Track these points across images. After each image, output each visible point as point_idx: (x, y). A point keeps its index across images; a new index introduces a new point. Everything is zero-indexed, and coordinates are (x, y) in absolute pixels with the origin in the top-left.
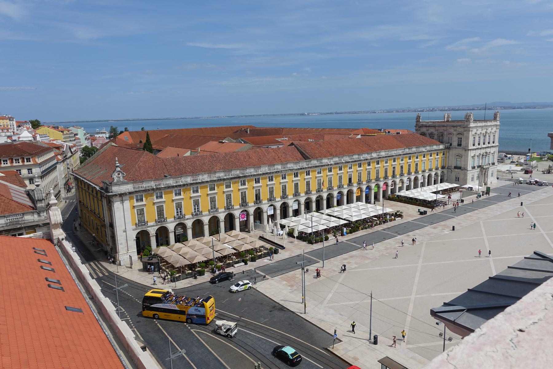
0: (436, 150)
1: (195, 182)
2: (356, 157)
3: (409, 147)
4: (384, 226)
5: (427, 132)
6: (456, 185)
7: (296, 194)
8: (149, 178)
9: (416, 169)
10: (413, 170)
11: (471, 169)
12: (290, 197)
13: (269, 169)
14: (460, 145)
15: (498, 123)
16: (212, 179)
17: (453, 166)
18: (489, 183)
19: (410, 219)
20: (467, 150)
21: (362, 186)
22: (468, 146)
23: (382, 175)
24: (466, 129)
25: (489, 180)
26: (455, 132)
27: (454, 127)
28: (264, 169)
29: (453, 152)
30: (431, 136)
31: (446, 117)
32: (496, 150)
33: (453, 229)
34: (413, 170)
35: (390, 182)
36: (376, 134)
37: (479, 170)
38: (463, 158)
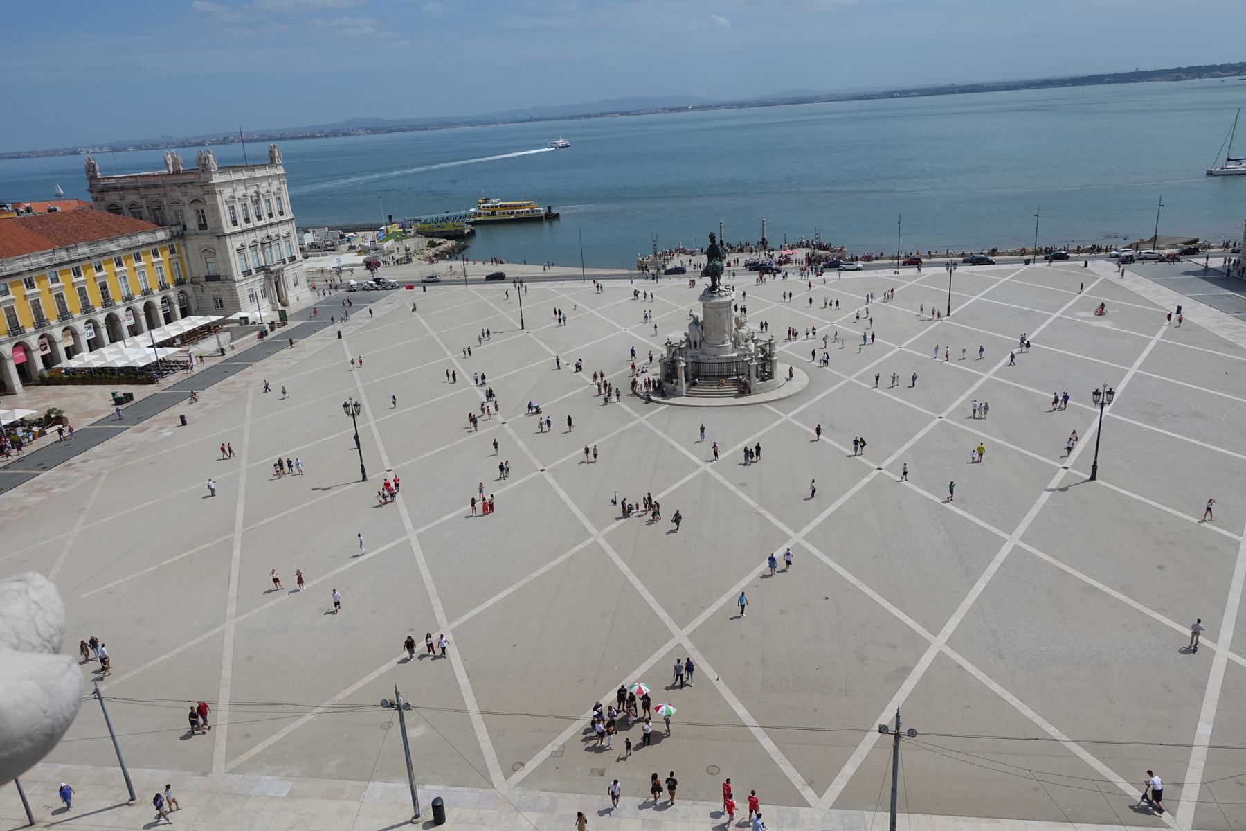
0: (147, 245)
3: (67, 245)
5: (122, 204)
6: (214, 318)
9: (105, 295)
10: (95, 298)
11: (242, 277)
14: (203, 226)
15: (281, 170)
17: (202, 275)
22: (221, 228)
24: (206, 189)
25: (290, 294)
26: (185, 199)
27: (180, 185)
29: (194, 245)
30: (135, 210)
31: (170, 162)
32: (291, 227)
33: (184, 423)
34: (95, 298)
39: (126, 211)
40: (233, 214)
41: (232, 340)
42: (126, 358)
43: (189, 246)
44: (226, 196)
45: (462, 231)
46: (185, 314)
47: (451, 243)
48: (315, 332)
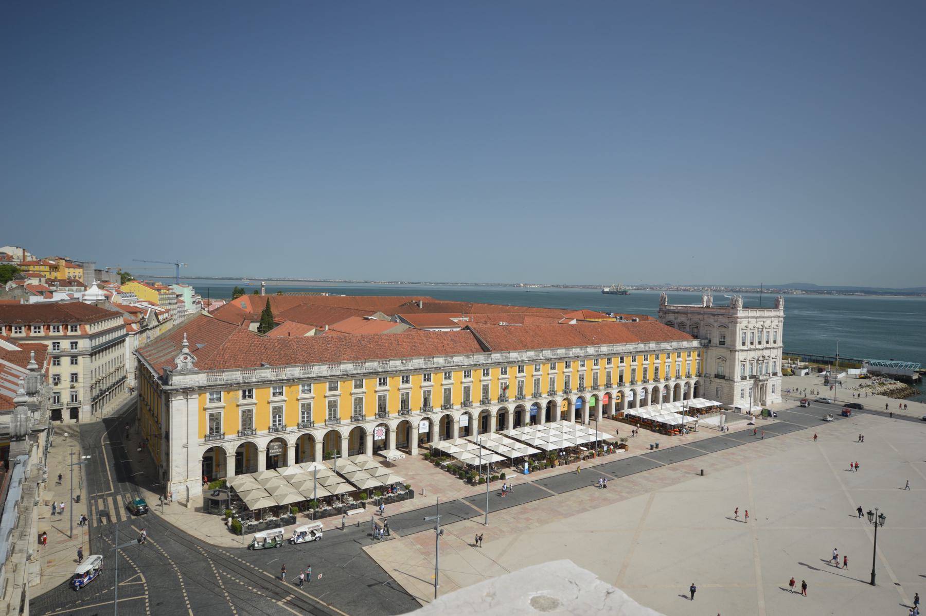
1: (306, 376)
2: (561, 352)
3: (645, 340)
4: (597, 461)
6: (716, 403)
7: (466, 403)
8: (236, 367)
9: (656, 374)
10: (650, 375)
12: (457, 406)
13: (426, 363)
15: (781, 313)
16: (333, 373)
18: (768, 403)
19: (638, 453)
20: (733, 350)
22: (734, 345)
23: (602, 381)
24: (731, 319)
25: (768, 398)
26: (715, 324)
27: (714, 315)
28: (418, 362)
29: (714, 352)
30: (681, 326)
32: (779, 353)
34: (650, 375)
35: (614, 392)
36: (600, 320)
37: (752, 381)
38: (728, 362)
41: (726, 421)
42: (649, 413)
45: (911, 378)
46: (695, 397)
47: (900, 385)
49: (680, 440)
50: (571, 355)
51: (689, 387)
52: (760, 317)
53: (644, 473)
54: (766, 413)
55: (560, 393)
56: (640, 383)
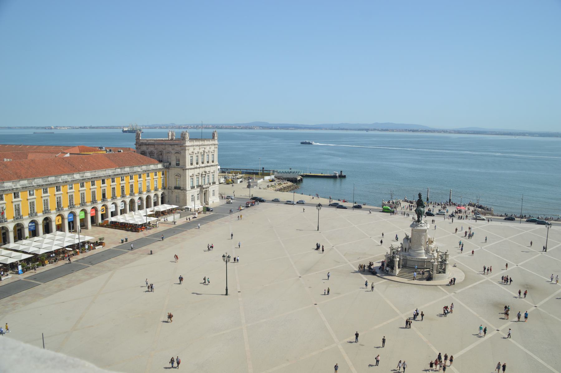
2: (52, 179)
3: (121, 166)
4: (80, 256)
5: (147, 151)
6: (174, 207)
9: (132, 191)
10: (127, 191)
11: (190, 189)
14: (178, 165)
15: (216, 142)
18: (210, 203)
19: (112, 246)
20: (184, 169)
21: (62, 213)
22: (185, 166)
24: (182, 148)
27: (171, 145)
29: (173, 171)
30: (151, 154)
31: (170, 135)
34: (127, 191)
35: (99, 207)
36: (91, 153)
37: (199, 189)
39: (148, 154)
40: (192, 160)
43: (170, 173)
44: (190, 151)
45: (296, 179)
46: (162, 203)
47: (290, 184)
48: (218, 219)
49: (145, 234)
50: (60, 181)
51: (158, 197)
52: (202, 145)
53: (112, 259)
54: (208, 209)
55: (53, 211)
56: (119, 198)
